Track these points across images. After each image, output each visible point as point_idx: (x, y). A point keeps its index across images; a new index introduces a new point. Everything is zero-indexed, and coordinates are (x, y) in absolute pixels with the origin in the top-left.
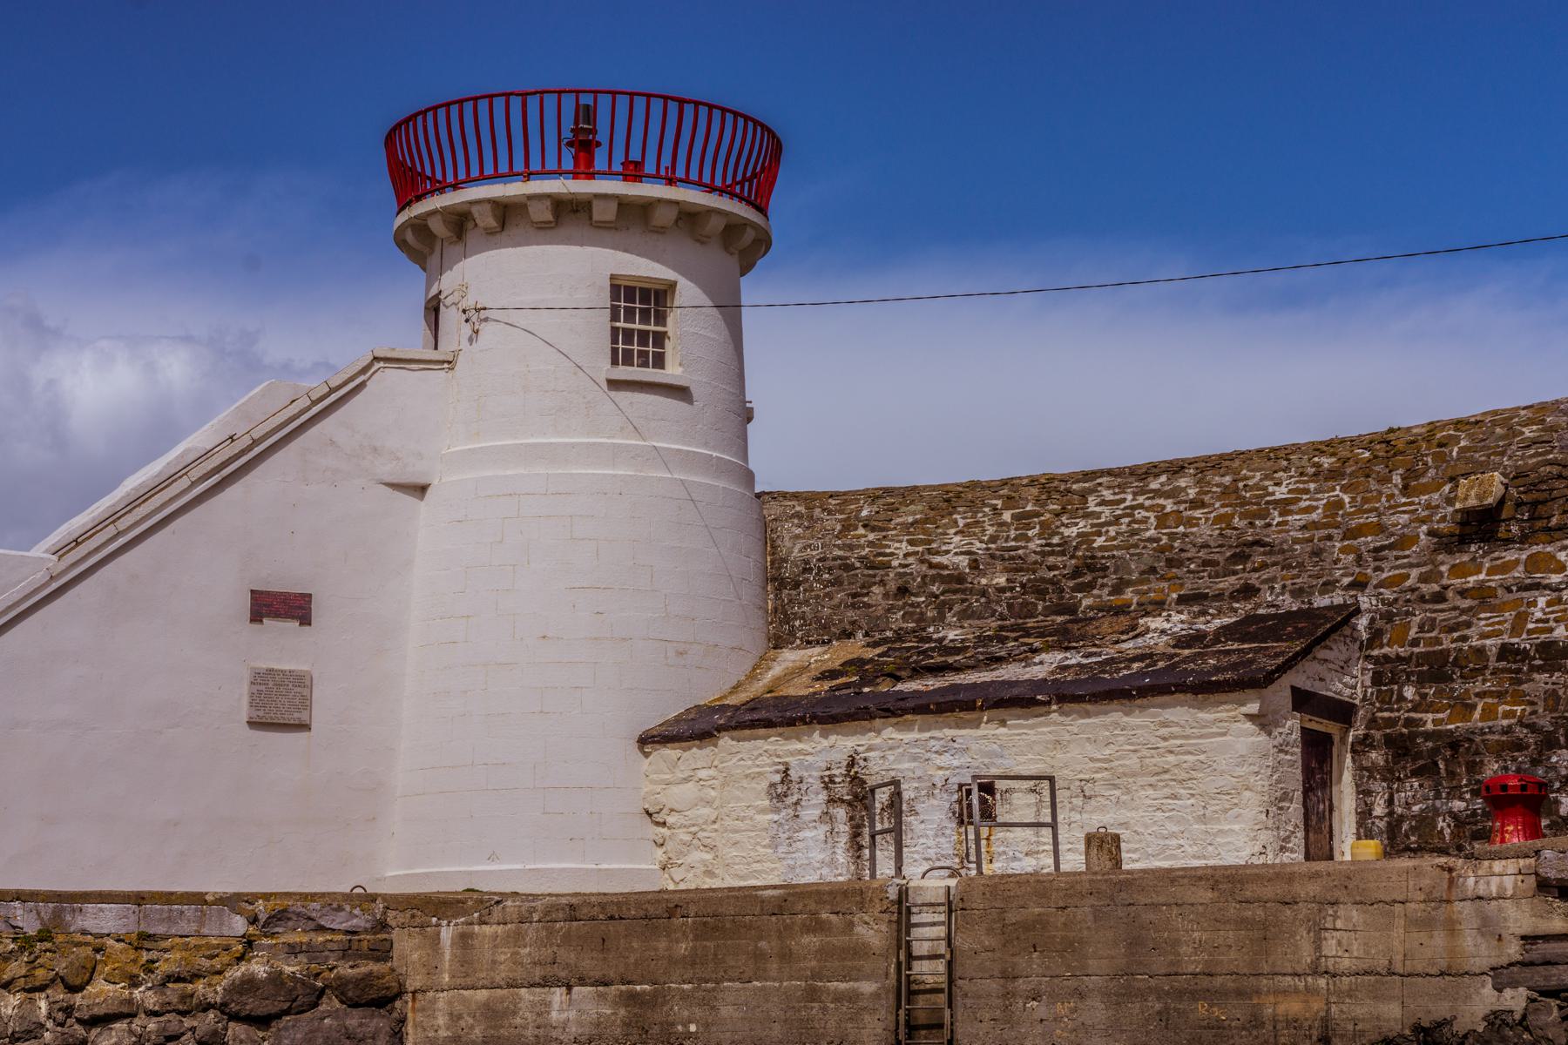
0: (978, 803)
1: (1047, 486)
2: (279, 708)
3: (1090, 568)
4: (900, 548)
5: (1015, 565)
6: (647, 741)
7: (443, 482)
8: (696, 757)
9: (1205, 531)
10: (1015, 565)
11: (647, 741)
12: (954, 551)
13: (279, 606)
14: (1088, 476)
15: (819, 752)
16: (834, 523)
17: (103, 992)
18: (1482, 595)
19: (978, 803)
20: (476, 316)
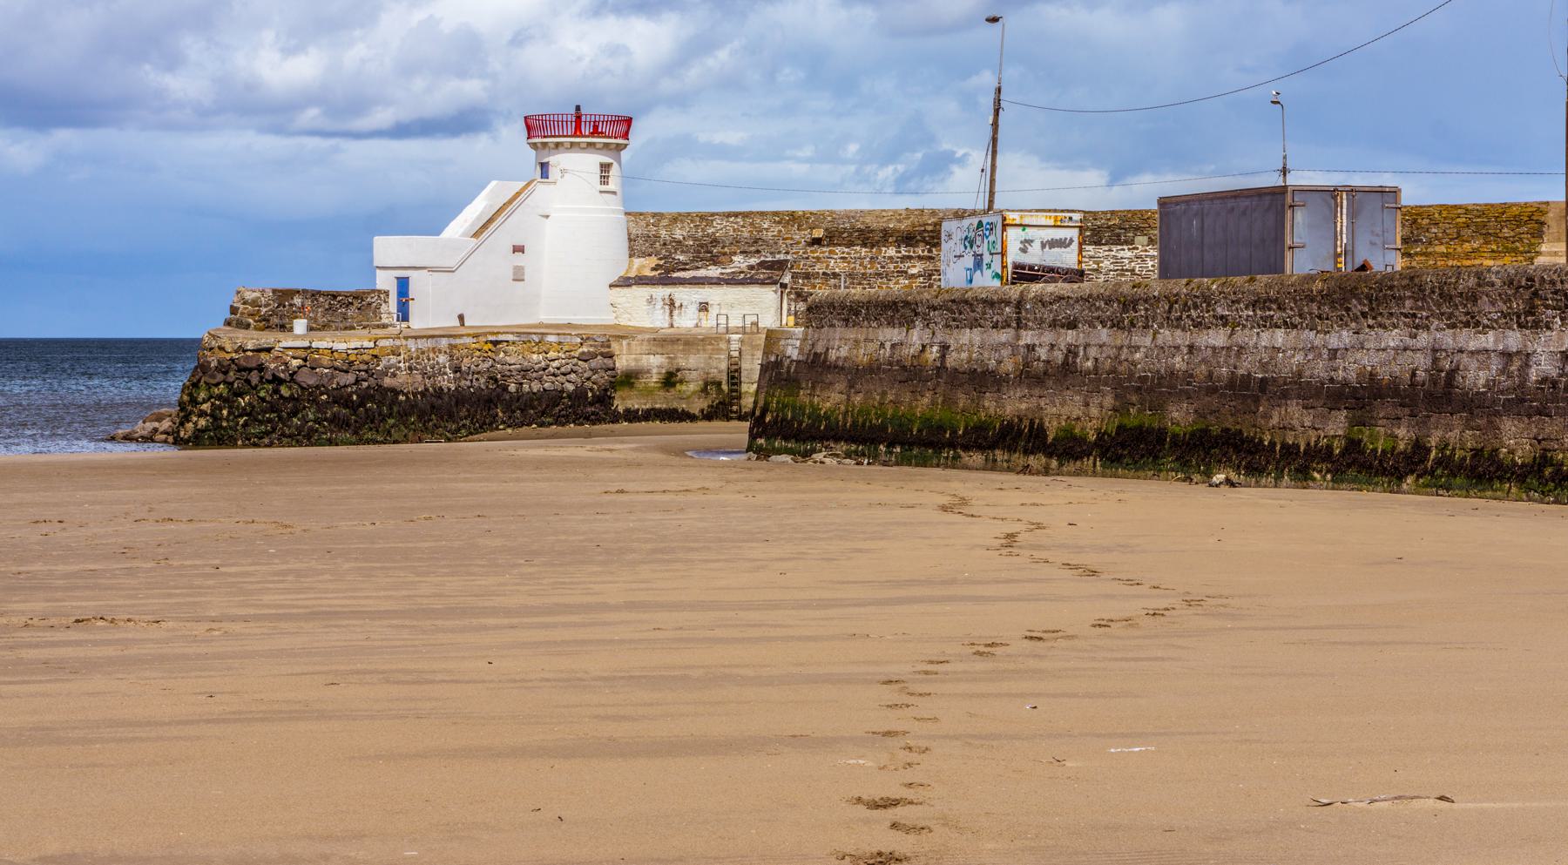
0: (704, 307)
1: (702, 217)
2: (518, 276)
3: (715, 241)
4: (663, 233)
5: (695, 239)
6: (611, 286)
7: (552, 215)
8: (626, 291)
9: (746, 234)
10: (695, 239)
11: (611, 286)
12: (679, 234)
13: (519, 249)
14: (713, 215)
15: (661, 292)
16: (643, 223)
17: (552, 355)
18: (818, 259)
19: (704, 307)
20: (563, 171)
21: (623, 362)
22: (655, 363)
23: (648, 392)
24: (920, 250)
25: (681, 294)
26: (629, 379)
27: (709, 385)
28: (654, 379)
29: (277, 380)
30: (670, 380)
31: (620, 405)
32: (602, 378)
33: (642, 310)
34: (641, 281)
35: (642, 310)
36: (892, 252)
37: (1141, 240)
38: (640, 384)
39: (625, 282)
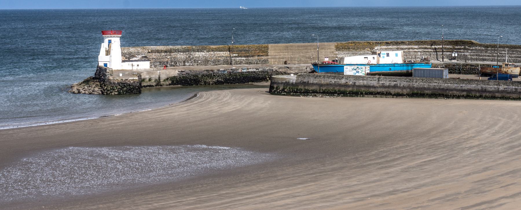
0: (138, 65)
15: (131, 63)
19: (138, 65)
21: (143, 77)
22: (147, 77)
23: (147, 82)
24: (168, 54)
25: (134, 63)
26: (144, 80)
27: (156, 80)
28: (147, 80)
29: (130, 85)
30: (150, 80)
31: (143, 85)
32: (140, 80)
33: (127, 66)
34: (127, 61)
35: (127, 66)
36: (163, 54)
37: (205, 51)
38: (145, 81)
39: (123, 61)
